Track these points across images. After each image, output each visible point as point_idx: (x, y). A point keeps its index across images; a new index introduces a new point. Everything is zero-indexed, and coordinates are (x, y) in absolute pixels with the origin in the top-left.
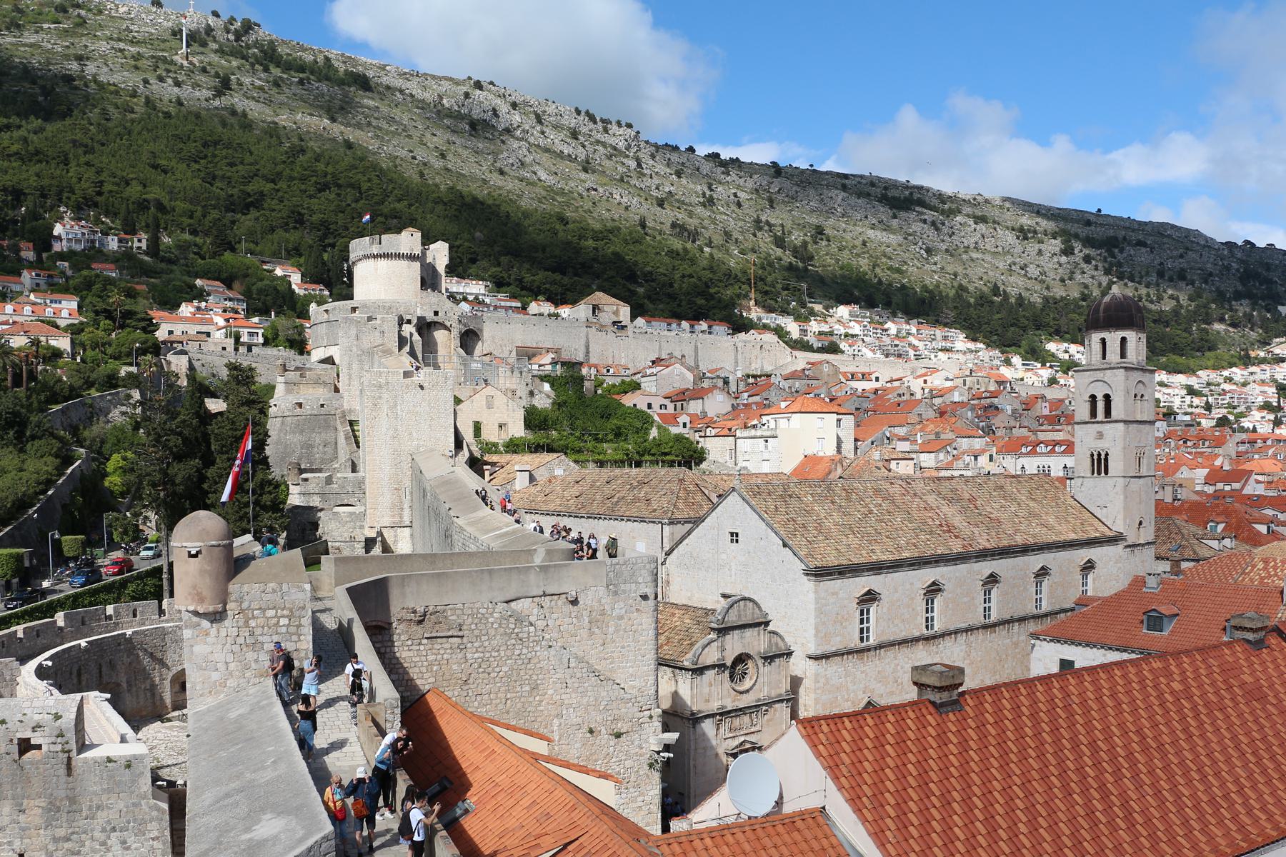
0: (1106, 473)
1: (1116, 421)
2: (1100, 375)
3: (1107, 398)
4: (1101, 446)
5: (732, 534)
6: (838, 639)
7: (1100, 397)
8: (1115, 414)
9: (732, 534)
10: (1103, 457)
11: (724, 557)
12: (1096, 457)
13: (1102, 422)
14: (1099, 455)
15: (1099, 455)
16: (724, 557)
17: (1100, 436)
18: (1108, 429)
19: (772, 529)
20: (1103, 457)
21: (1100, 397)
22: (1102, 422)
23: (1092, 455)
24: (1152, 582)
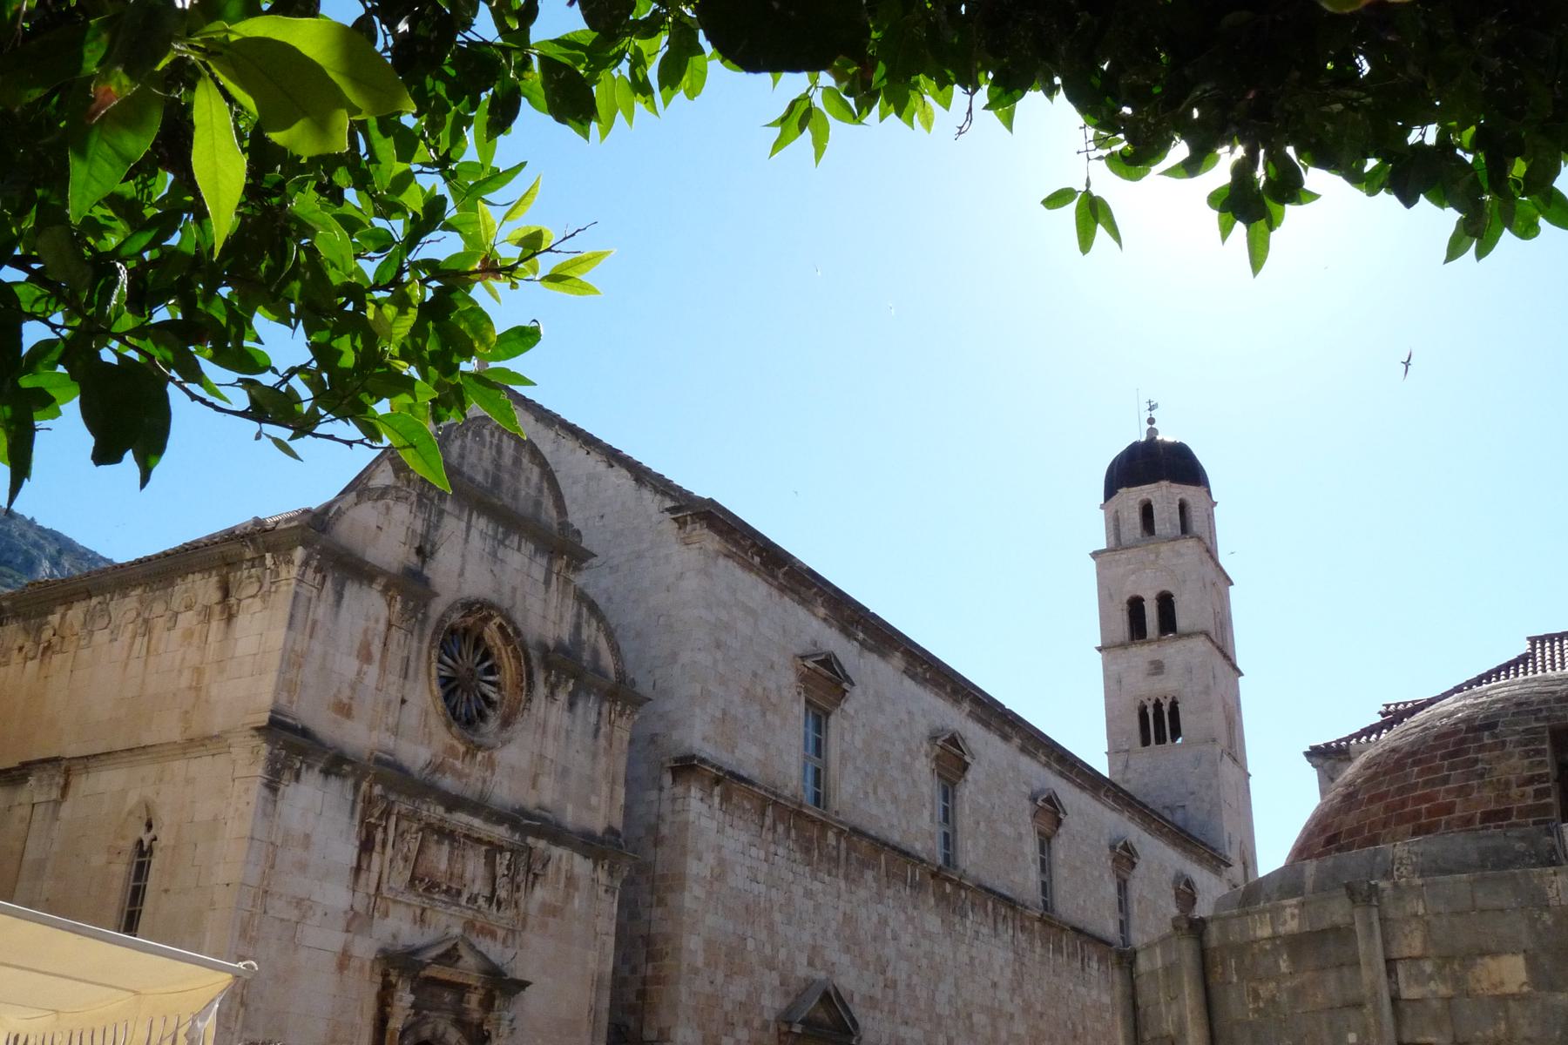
1: (1189, 635)
4: (1164, 687)
6: (754, 752)
8: (1182, 622)
10: (1166, 709)
12: (1150, 711)
14: (1158, 706)
15: (1158, 706)
17: (1157, 668)
18: (1172, 652)
20: (1166, 709)
22: (1159, 640)
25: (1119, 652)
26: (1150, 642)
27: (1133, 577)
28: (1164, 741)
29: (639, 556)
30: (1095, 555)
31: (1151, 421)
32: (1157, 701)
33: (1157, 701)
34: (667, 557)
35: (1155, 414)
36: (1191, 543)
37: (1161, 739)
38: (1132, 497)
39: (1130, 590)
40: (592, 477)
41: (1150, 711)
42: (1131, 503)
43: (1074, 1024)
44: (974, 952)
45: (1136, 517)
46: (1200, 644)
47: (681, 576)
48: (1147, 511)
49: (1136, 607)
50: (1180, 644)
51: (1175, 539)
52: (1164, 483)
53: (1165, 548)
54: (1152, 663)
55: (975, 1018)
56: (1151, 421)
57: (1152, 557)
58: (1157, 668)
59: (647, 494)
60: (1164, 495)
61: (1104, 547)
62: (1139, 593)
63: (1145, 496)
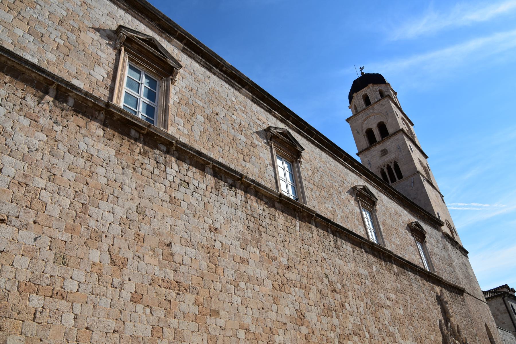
0: (400, 176)
1: (395, 134)
2: (370, 111)
3: (382, 127)
7: (374, 127)
10: (392, 167)
14: (389, 167)
15: (389, 167)
18: (390, 144)
20: (392, 167)
21: (374, 127)
22: (382, 140)
25: (366, 153)
26: (379, 143)
27: (366, 122)
28: (395, 180)
30: (348, 120)
32: (388, 165)
33: (388, 165)
35: (363, 71)
36: (386, 99)
37: (393, 180)
38: (359, 95)
39: (365, 127)
43: (330, 282)
44: (179, 195)
45: (362, 102)
46: (400, 135)
48: (367, 101)
49: (369, 133)
50: (392, 139)
51: (380, 100)
52: (370, 85)
53: (376, 106)
54: (382, 151)
55: (176, 248)
57: (371, 111)
58: (384, 152)
60: (371, 91)
61: (352, 115)
62: (370, 127)
63: (364, 93)
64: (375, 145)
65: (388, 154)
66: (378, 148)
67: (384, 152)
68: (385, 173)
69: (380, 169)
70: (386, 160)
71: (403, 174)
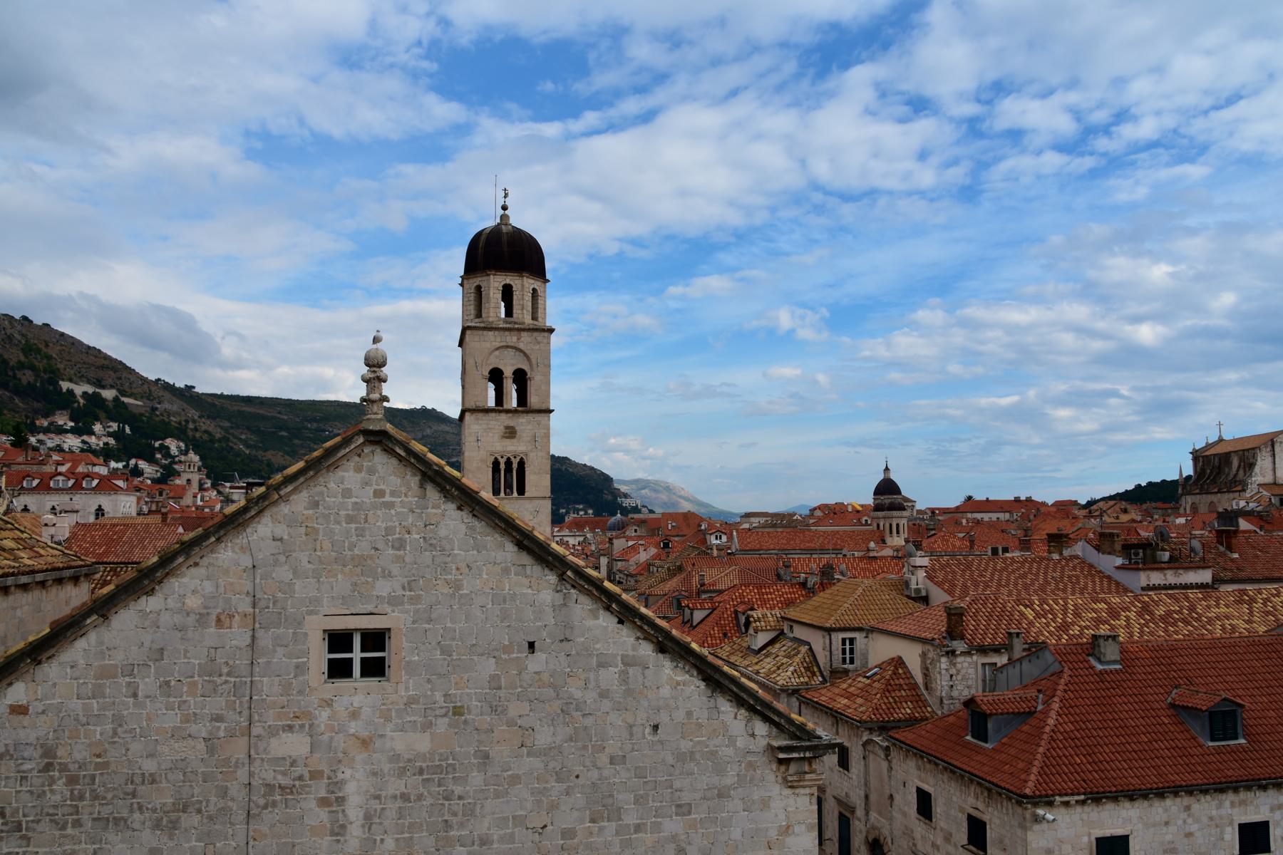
0: (521, 491)
2: (512, 339)
5: (338, 640)
7: (508, 372)
9: (338, 640)
10: (515, 466)
11: (294, 745)
12: (502, 466)
13: (514, 411)
14: (509, 463)
16: (294, 745)
17: (510, 433)
18: (524, 423)
19: (608, 601)
20: (515, 466)
21: (508, 372)
22: (514, 411)
23: (496, 464)
24: (1111, 651)
25: (480, 415)
26: (508, 411)
29: (722, 794)
31: (504, 208)
34: (765, 804)
38: (494, 283)
40: (628, 662)
41: (502, 466)
42: (496, 285)
47: (786, 830)
50: (530, 417)
54: (507, 428)
56: (504, 208)
57: (515, 339)
59: (726, 706)
60: (523, 285)
63: (508, 281)
64: (500, 412)
65: (514, 441)
66: (505, 420)
67: (510, 433)
68: (499, 471)
69: (492, 459)
70: (510, 448)
71: (527, 488)
